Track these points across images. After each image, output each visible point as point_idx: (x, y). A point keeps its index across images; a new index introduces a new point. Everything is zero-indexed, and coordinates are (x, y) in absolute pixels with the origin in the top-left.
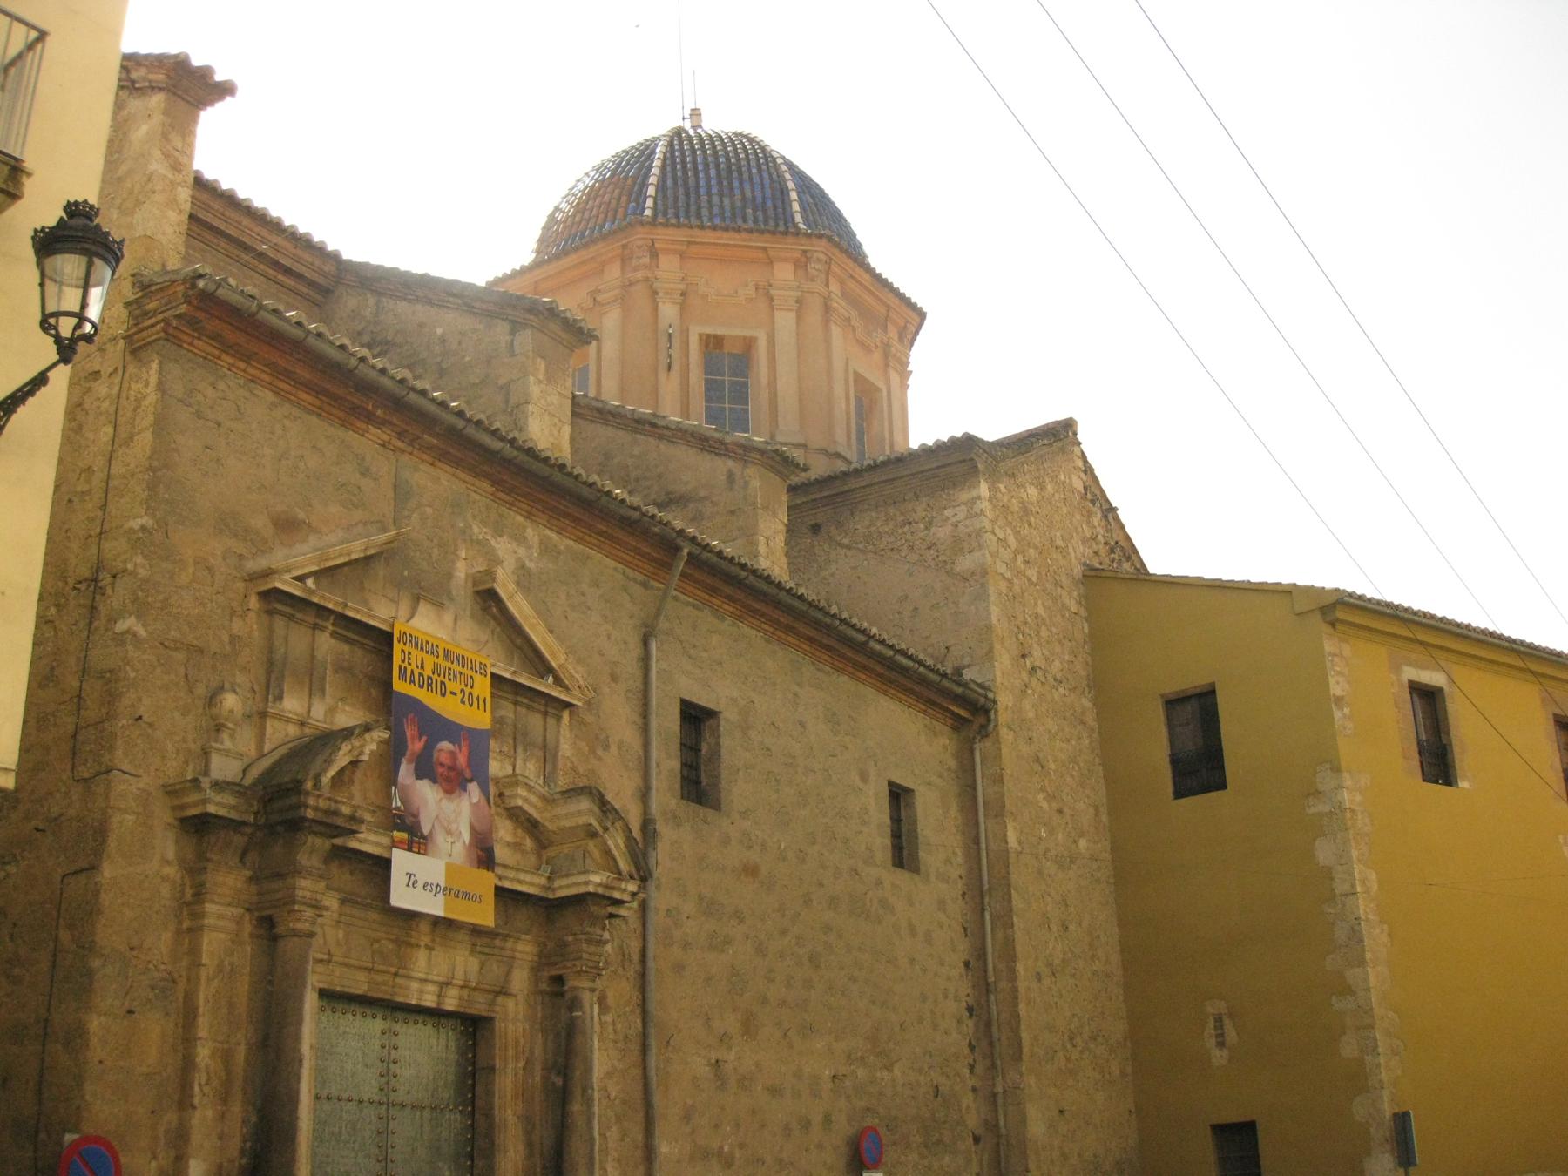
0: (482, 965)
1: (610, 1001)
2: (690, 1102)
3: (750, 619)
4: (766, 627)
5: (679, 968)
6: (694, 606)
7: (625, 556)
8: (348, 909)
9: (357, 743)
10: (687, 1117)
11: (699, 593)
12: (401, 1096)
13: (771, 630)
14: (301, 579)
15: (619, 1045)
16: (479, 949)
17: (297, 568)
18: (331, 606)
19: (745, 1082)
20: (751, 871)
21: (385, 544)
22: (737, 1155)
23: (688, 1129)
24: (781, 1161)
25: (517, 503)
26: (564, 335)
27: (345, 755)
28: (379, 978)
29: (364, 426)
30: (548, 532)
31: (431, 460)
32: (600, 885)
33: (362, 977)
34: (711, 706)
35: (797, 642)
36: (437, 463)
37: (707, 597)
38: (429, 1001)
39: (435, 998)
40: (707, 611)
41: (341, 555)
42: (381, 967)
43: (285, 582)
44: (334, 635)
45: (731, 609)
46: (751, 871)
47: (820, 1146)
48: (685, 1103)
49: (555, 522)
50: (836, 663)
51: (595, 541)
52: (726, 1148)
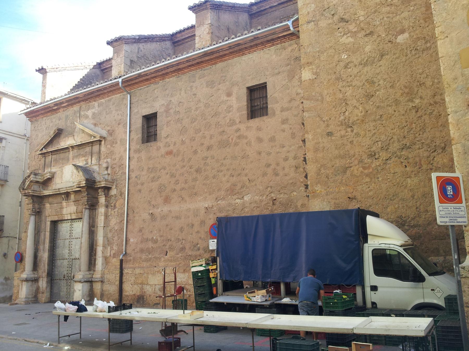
0: (77, 207)
1: (117, 206)
2: (142, 226)
3: (167, 76)
4: (174, 74)
5: (140, 191)
6: (147, 87)
7: (120, 91)
8: (51, 205)
9: (29, 179)
10: (140, 231)
11: (145, 83)
12: (74, 237)
13: (176, 73)
14: (42, 149)
15: (119, 216)
16: (76, 205)
17: (39, 149)
18: (46, 152)
19: (164, 217)
20: (170, 153)
21: (54, 134)
22: (159, 239)
23: (141, 234)
24: (179, 239)
25: (90, 101)
26: (118, 43)
27: (28, 182)
28: (59, 216)
29: (58, 111)
30: (101, 100)
31: (71, 107)
32: (76, 185)
33: (56, 217)
34: (154, 112)
35: (189, 69)
36: (73, 106)
37: (149, 82)
38: (69, 218)
39: (70, 217)
40: (152, 85)
41: (46, 141)
42: (58, 214)
43: (39, 152)
44: (52, 155)
45: (159, 79)
46: (170, 153)
47: (198, 232)
48: (140, 227)
49: (100, 98)
50: (210, 63)
51: (111, 94)
52: (154, 238)
